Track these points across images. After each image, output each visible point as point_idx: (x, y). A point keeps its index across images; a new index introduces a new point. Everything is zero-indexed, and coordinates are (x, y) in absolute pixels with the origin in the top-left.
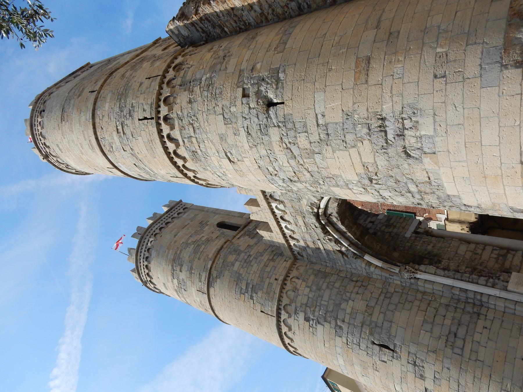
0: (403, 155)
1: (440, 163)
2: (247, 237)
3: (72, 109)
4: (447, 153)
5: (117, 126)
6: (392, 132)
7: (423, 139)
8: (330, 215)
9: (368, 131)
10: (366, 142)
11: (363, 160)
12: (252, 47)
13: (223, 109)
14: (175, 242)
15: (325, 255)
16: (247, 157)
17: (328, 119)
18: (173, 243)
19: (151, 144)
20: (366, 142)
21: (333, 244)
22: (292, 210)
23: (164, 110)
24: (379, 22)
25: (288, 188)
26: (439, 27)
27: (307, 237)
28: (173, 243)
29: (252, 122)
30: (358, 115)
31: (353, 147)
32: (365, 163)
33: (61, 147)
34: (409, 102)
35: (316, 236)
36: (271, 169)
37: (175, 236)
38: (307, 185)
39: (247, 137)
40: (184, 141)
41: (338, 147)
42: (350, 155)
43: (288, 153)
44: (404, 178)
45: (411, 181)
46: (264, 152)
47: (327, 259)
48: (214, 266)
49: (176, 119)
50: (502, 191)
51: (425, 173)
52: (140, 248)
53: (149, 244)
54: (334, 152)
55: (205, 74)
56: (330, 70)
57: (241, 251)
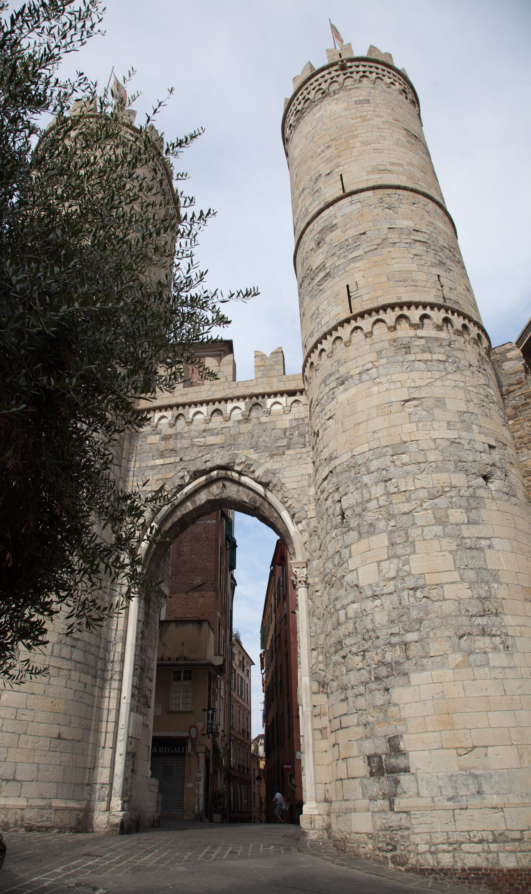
0: (461, 632)
1: (458, 670)
3: (422, 158)
4: (472, 678)
5: (421, 232)
6: (485, 623)
7: (484, 655)
8: (224, 486)
9: (483, 597)
10: (468, 593)
11: (445, 586)
13: (473, 413)
15: (151, 463)
16: (418, 430)
17: (488, 552)
19: (411, 283)
20: (468, 593)
21: (178, 482)
22: (233, 431)
25: (363, 469)
27: (185, 443)
29: (468, 452)
30: (498, 588)
31: (461, 576)
32: (442, 587)
33: (366, 107)
34: (517, 643)
35: (189, 458)
36: (405, 458)
38: (382, 503)
39: (447, 439)
40: (421, 338)
41: (458, 558)
42: (450, 571)
43: (438, 492)
44: (428, 630)
45: (425, 636)
46: (431, 457)
47: (143, 465)
50: (430, 728)
51: (441, 653)
54: (450, 551)
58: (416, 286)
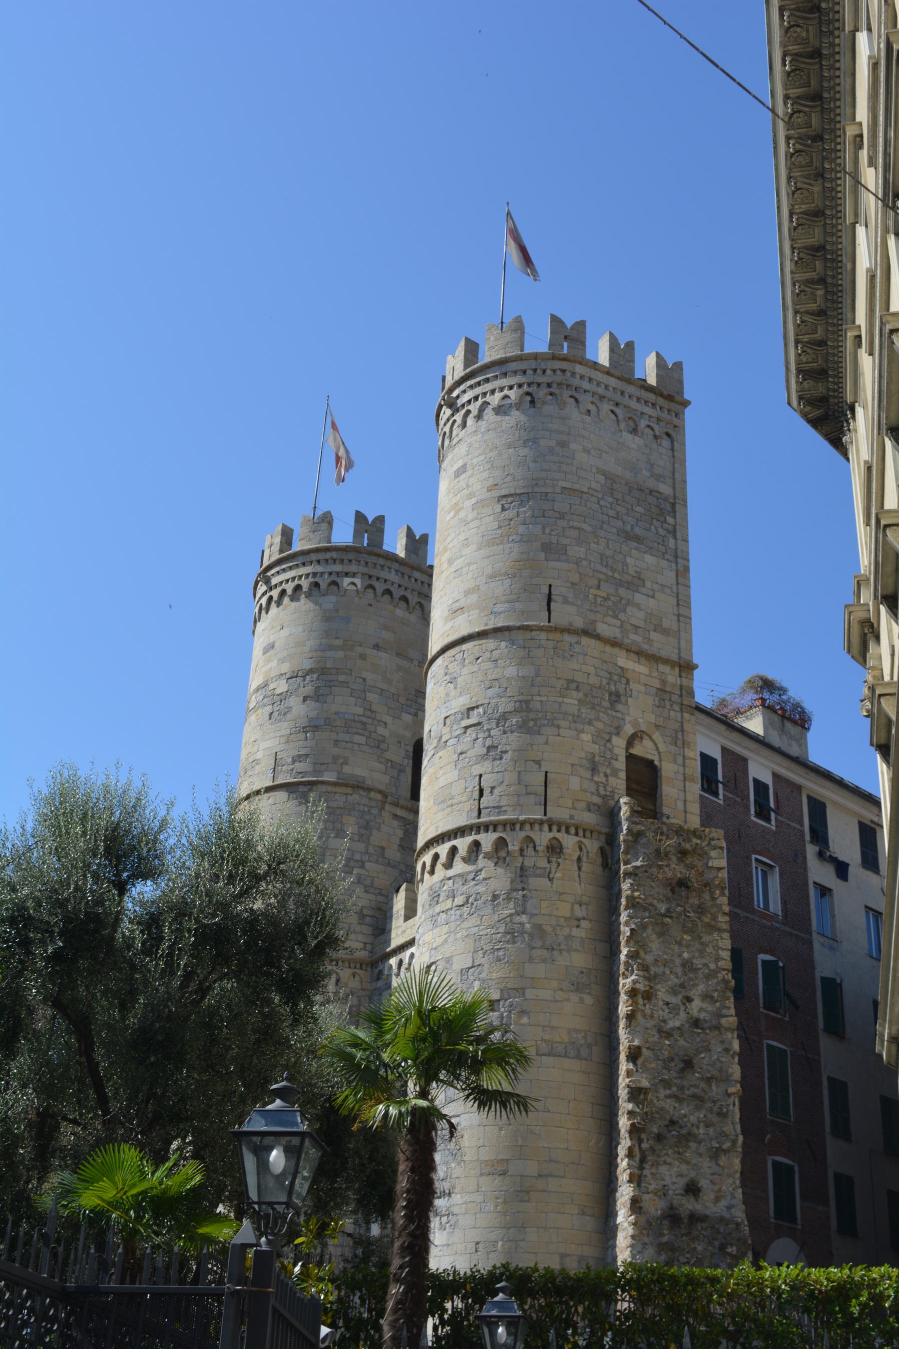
2: (400, 833)
12: (560, 995)
14: (363, 657)
18: (359, 650)
23: (487, 840)
24: (547, 1176)
26: (523, 1240)
28: (359, 650)
37: (376, 647)
48: (329, 788)
49: (475, 867)
52: (334, 555)
53: (347, 581)
55: (532, 915)
56: (501, 1129)
57: (368, 839)
58: (452, 805)
